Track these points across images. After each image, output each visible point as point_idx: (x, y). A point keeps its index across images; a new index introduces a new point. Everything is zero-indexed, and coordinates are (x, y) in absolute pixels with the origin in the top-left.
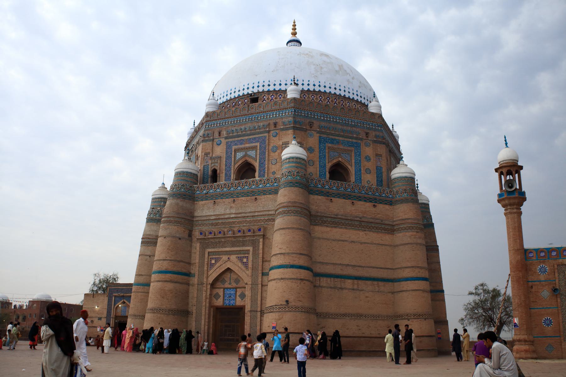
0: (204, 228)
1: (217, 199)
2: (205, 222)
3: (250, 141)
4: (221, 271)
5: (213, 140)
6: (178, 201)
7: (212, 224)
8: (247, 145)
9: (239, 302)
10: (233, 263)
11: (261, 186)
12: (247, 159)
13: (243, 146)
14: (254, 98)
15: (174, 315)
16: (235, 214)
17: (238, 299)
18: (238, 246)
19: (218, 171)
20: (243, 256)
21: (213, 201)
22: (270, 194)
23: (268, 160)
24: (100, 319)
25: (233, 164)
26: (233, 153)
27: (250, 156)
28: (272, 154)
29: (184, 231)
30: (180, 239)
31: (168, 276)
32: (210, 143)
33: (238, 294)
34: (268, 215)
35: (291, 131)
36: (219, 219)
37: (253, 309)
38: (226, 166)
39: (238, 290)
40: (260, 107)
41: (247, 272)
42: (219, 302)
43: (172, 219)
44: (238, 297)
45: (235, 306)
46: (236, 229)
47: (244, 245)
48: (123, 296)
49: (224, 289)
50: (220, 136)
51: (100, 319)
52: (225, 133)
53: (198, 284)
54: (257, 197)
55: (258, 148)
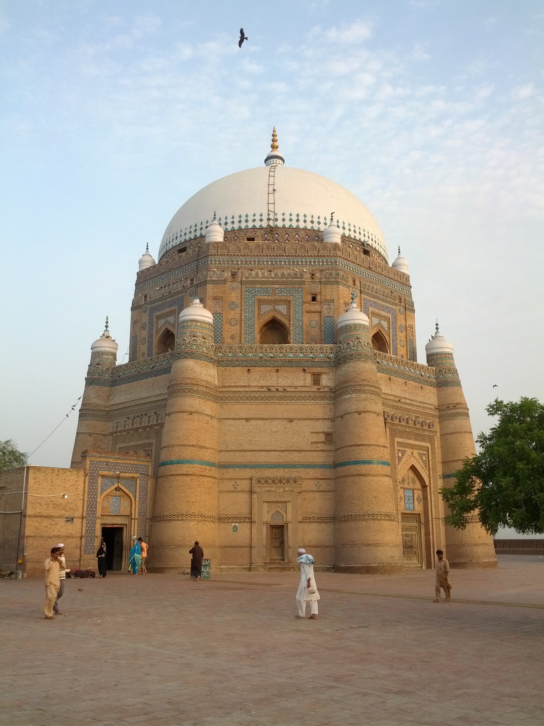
1: (392, 375)
3: (383, 308)
13: (376, 311)
14: (367, 250)
20: (422, 452)
21: (387, 376)
24: (70, 520)
47: (423, 440)
48: (118, 477)
50: (354, 285)
51: (70, 520)
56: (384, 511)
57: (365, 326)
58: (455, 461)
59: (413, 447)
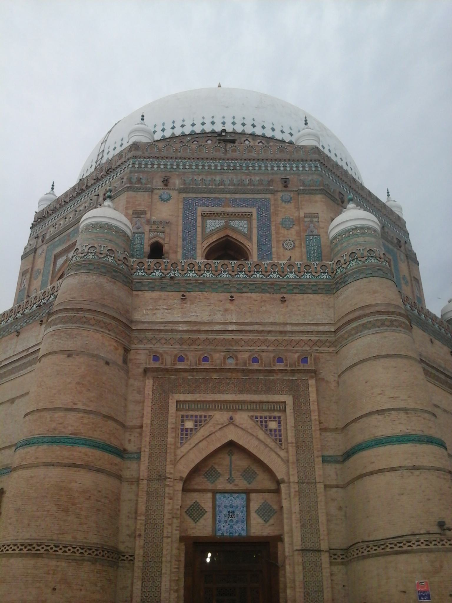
0: (160, 348)
2: (162, 335)
3: (234, 202)
4: (212, 448)
5: (152, 191)
6: (102, 280)
7: (182, 342)
8: (231, 210)
9: (259, 528)
10: (244, 430)
11: (291, 276)
12: (231, 234)
15: (94, 562)
16: (236, 323)
17: (256, 520)
18: (256, 392)
19: (166, 248)
20: (267, 414)
22: (315, 292)
23: (278, 241)
25: (199, 237)
26: (199, 219)
27: (234, 230)
28: (283, 231)
29: (116, 349)
30: (107, 363)
31: (81, 453)
32: (146, 194)
33: (254, 506)
34: (318, 332)
35: (320, 196)
36: (199, 331)
37: (309, 546)
38: (184, 240)
39: (253, 496)
40: (250, 151)
41: (282, 454)
42: (203, 528)
43: (87, 315)
44: (253, 515)
45: (249, 537)
46: (246, 356)
47: (269, 390)
49: (215, 492)
50: (166, 185)
52: (177, 182)
53: (149, 480)
54: (284, 295)
55: (255, 216)
56: (28, 536)
57: (97, 224)
58: (355, 420)
59: (234, 407)
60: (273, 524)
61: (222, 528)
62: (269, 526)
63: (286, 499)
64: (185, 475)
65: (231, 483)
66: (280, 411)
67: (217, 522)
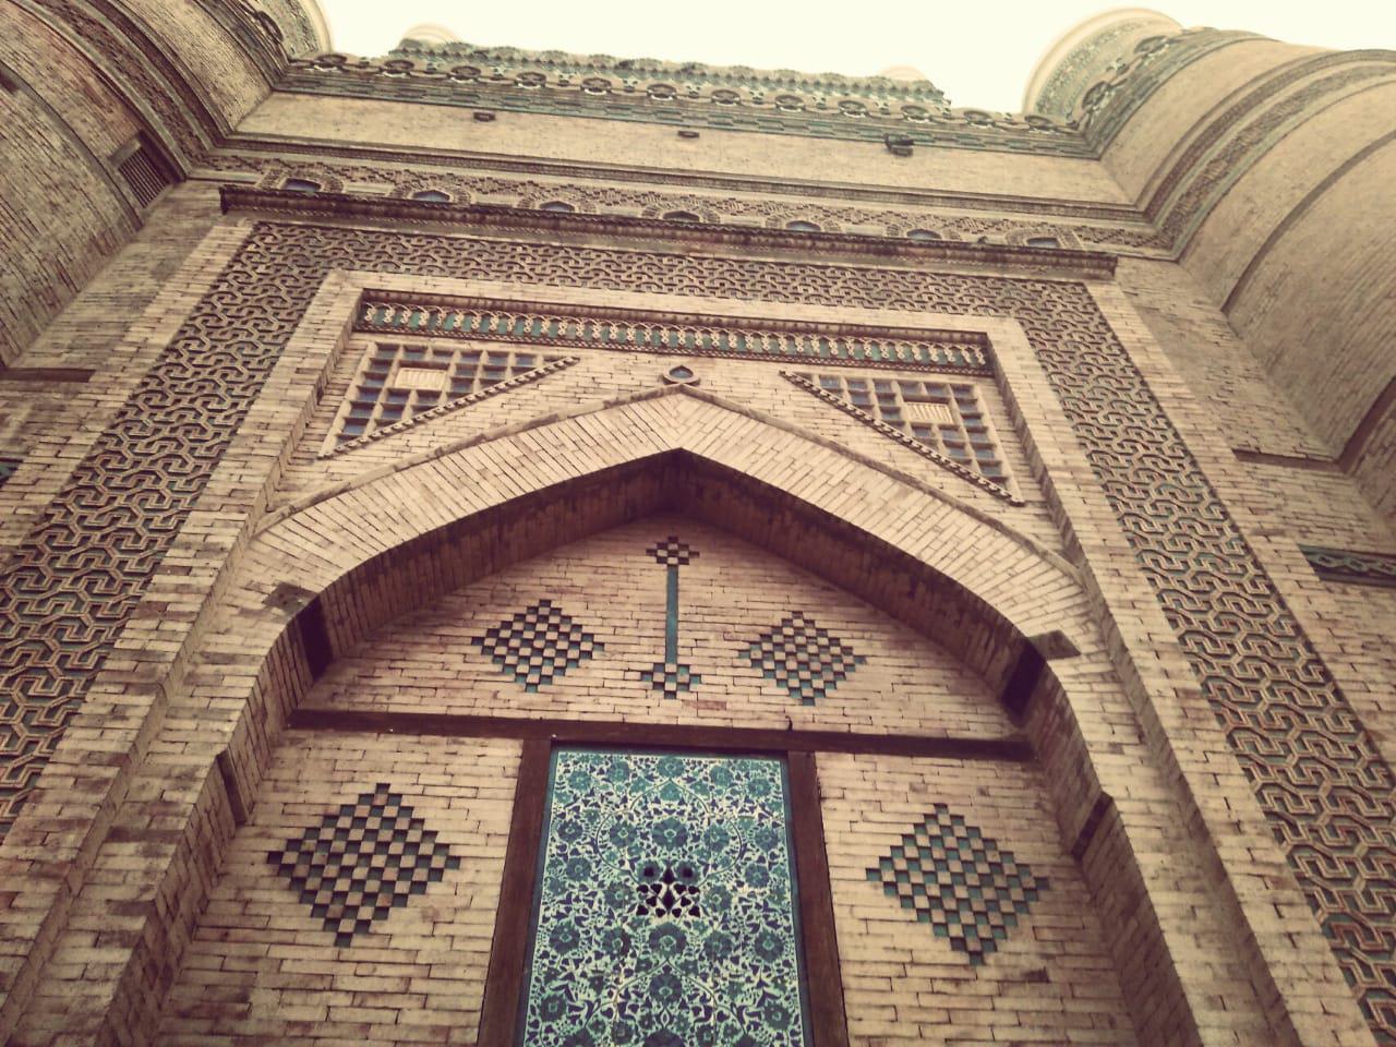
39: (835, 770)
49: (543, 740)
60: (1039, 977)
61: (583, 995)
62: (1004, 985)
63: (1116, 748)
64: (318, 582)
65: (671, 695)
66: (960, 368)
67: (542, 943)
